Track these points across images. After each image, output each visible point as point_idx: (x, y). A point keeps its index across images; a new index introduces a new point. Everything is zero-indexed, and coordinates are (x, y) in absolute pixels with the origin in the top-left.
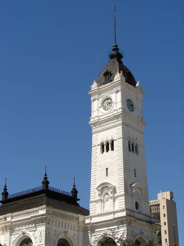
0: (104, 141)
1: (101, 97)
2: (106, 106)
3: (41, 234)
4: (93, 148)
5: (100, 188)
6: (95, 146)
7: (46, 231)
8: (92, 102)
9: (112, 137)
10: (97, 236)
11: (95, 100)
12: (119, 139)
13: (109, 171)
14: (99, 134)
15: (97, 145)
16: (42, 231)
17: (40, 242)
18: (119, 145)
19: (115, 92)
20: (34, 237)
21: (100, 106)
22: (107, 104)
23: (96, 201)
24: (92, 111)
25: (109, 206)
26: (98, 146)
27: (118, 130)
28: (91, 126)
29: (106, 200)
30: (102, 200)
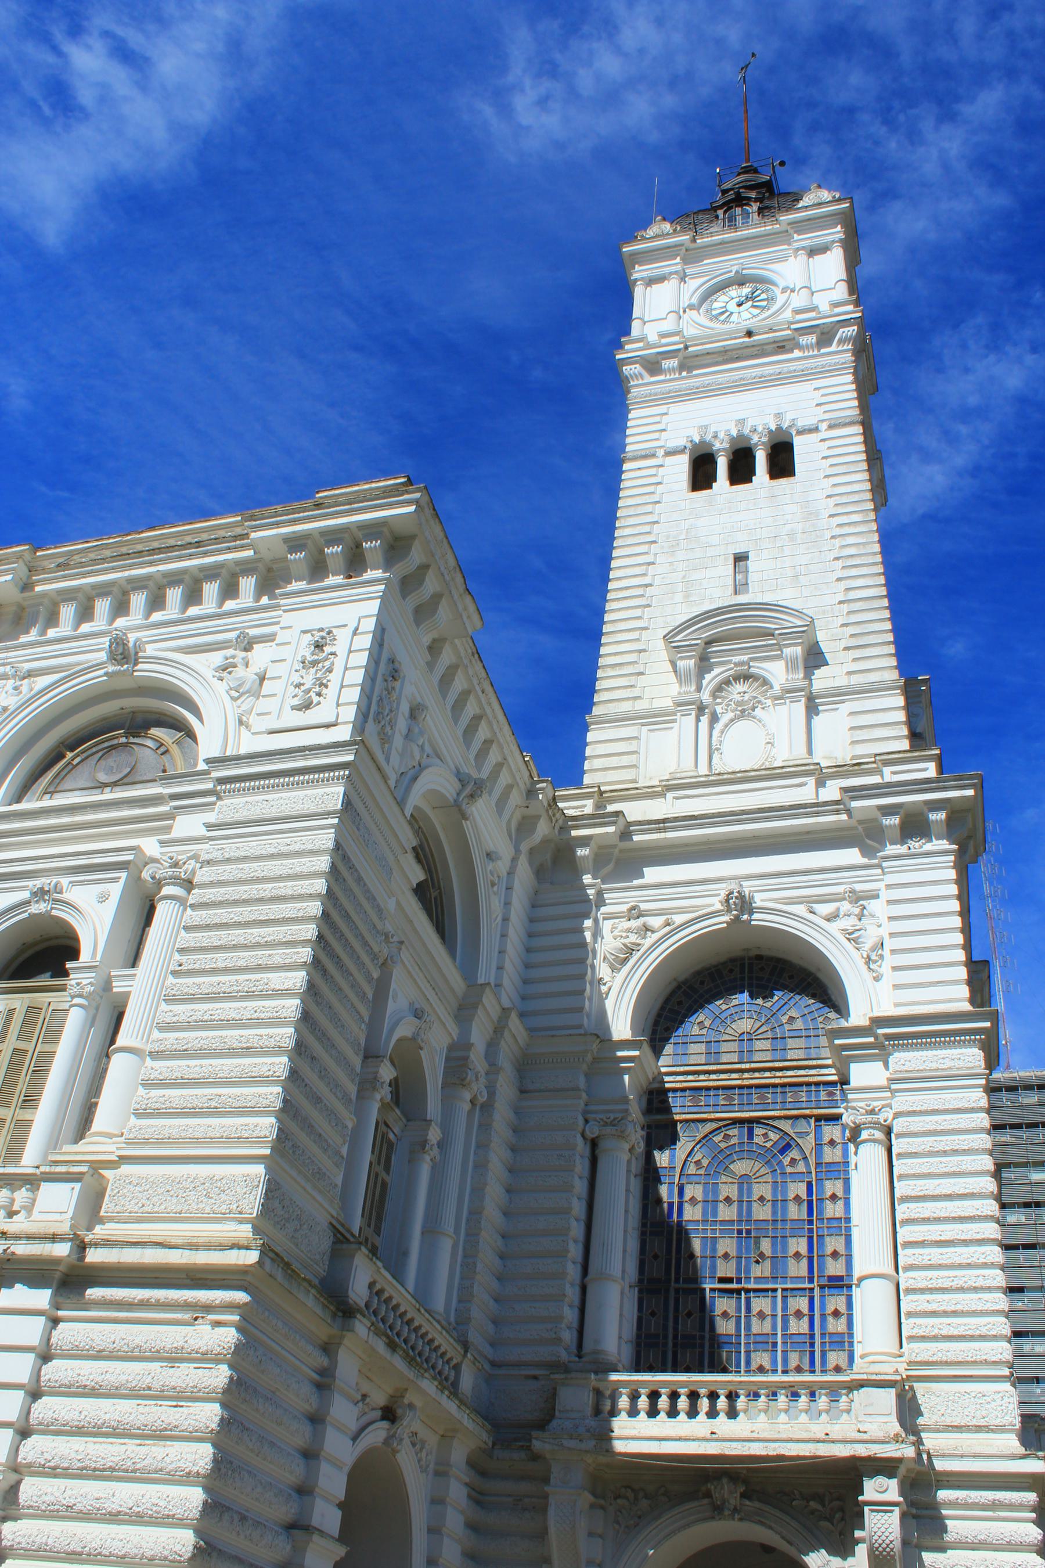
0: (722, 435)
1: (695, 276)
2: (732, 306)
3: (328, 649)
4: (625, 467)
5: (697, 636)
6: (654, 456)
7: (375, 659)
8: (639, 291)
9: (778, 415)
10: (656, 922)
11: (651, 282)
12: (831, 427)
13: (752, 564)
14: (674, 408)
15: (661, 452)
16: (343, 637)
17: (307, 706)
18: (833, 463)
19: (803, 248)
20: (221, 687)
21: (694, 300)
22: (737, 300)
23: (656, 718)
24: (636, 313)
25: (767, 734)
26: (669, 453)
27: (823, 392)
28: (627, 370)
29: (731, 715)
30: (701, 709)
